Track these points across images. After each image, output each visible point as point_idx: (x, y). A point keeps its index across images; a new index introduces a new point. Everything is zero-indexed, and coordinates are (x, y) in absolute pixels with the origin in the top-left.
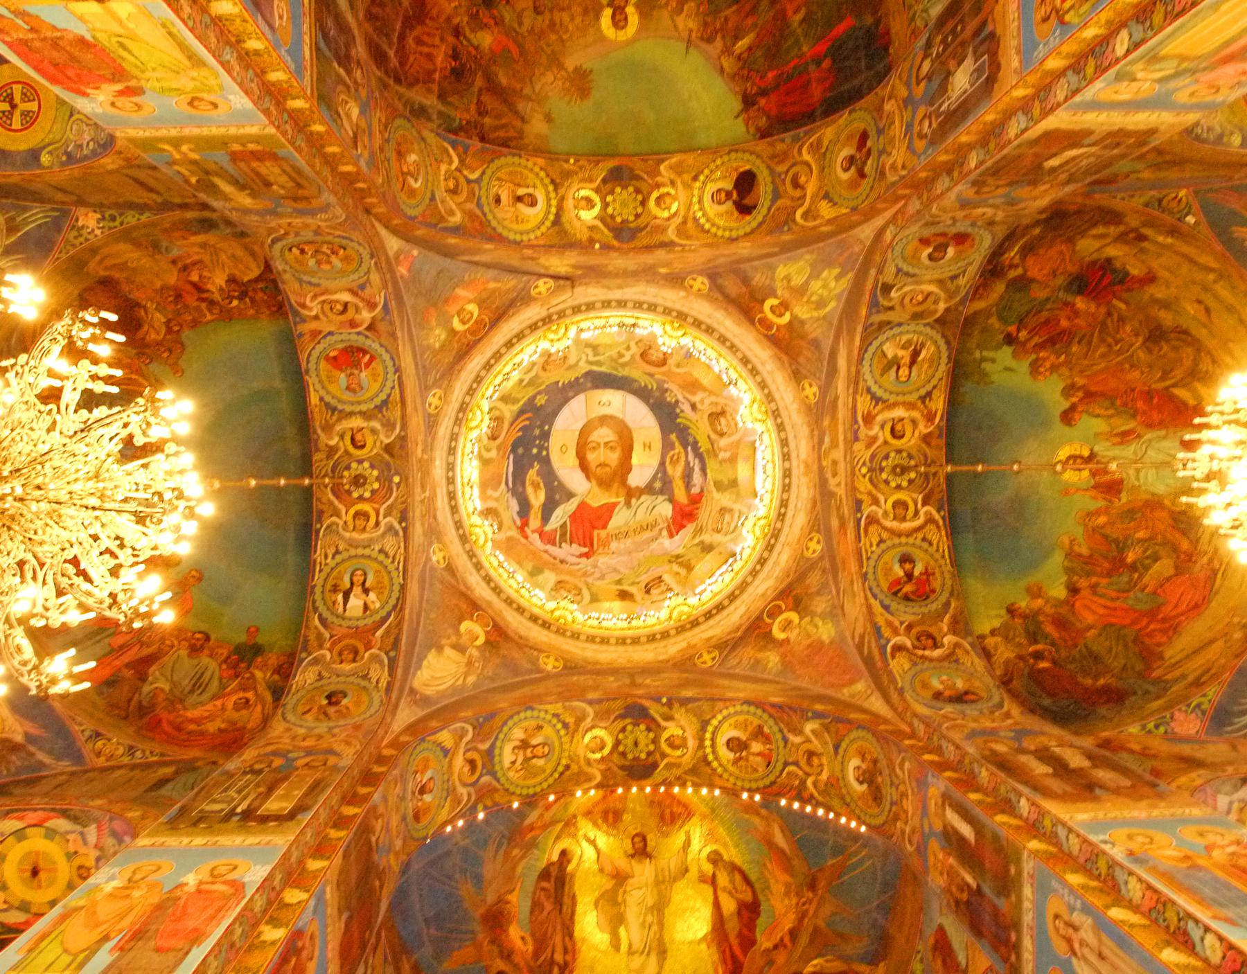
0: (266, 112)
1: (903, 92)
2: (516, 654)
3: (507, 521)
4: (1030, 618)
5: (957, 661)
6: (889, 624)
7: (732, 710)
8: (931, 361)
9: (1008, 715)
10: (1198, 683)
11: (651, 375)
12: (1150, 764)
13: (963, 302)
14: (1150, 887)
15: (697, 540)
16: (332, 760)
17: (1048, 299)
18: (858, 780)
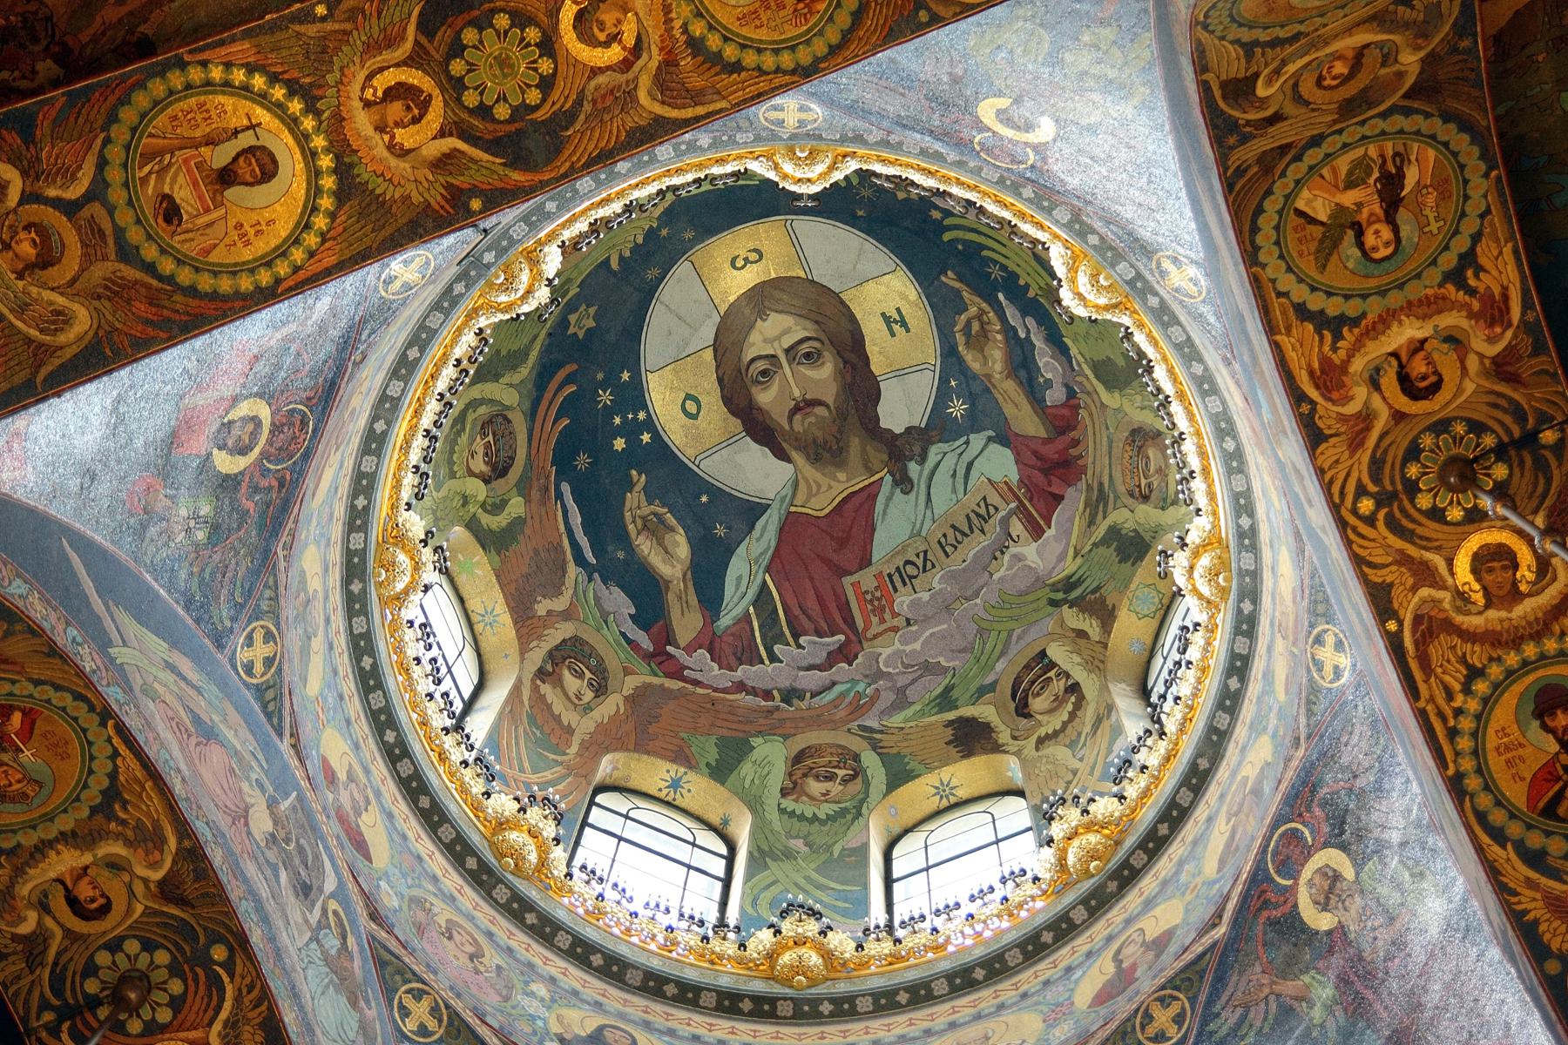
3: (613, 656)
8: (1441, 185)
15: (1100, 531)
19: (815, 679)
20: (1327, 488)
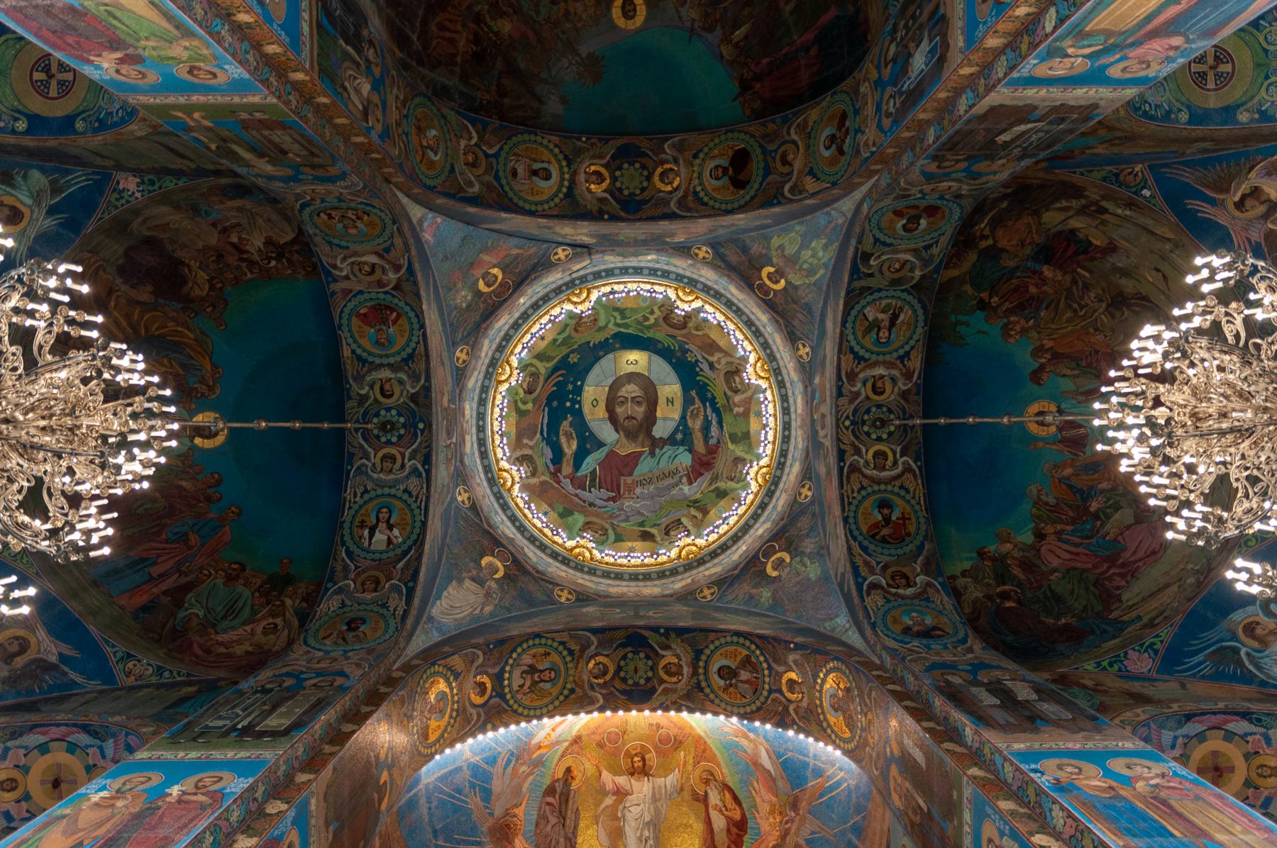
0: (265, 82)
1: (874, 75)
2: (532, 587)
3: (541, 468)
4: (1000, 562)
5: (928, 600)
6: (867, 563)
7: (723, 641)
9: (970, 650)
10: (1152, 624)
11: (673, 337)
12: (1099, 698)
13: (936, 270)
14: (1070, 815)
16: (339, 681)
17: (1017, 268)
18: (833, 707)
20: (837, 412)
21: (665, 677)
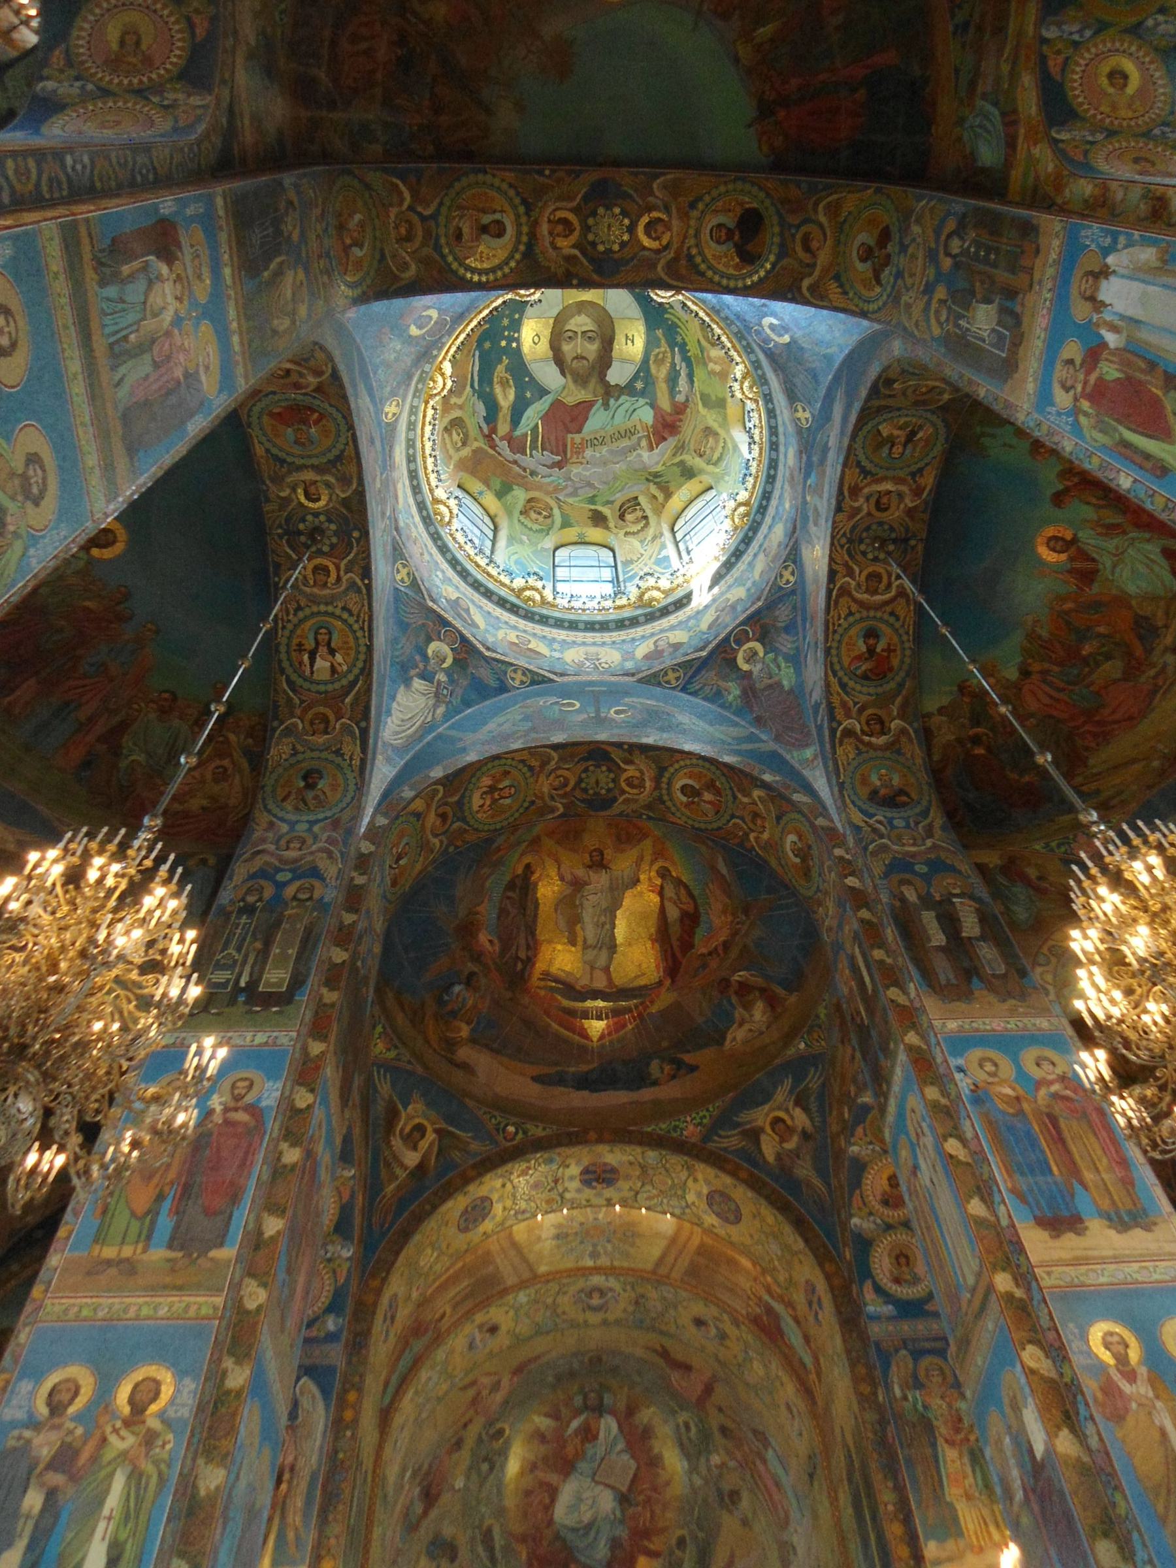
3: (473, 432)
7: (688, 762)
19: (546, 471)
21: (627, 789)
